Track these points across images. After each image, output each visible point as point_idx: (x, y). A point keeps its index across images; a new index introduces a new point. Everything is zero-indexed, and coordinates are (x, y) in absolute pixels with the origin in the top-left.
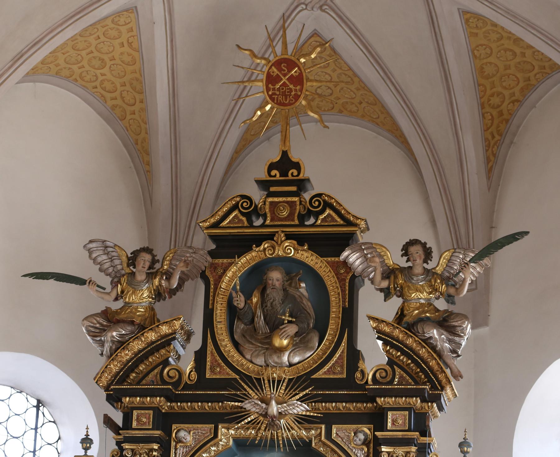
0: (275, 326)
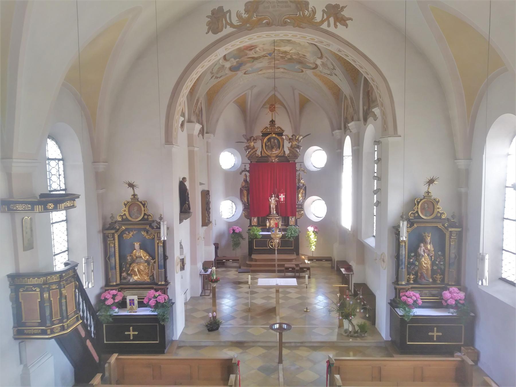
0: (272, 148)
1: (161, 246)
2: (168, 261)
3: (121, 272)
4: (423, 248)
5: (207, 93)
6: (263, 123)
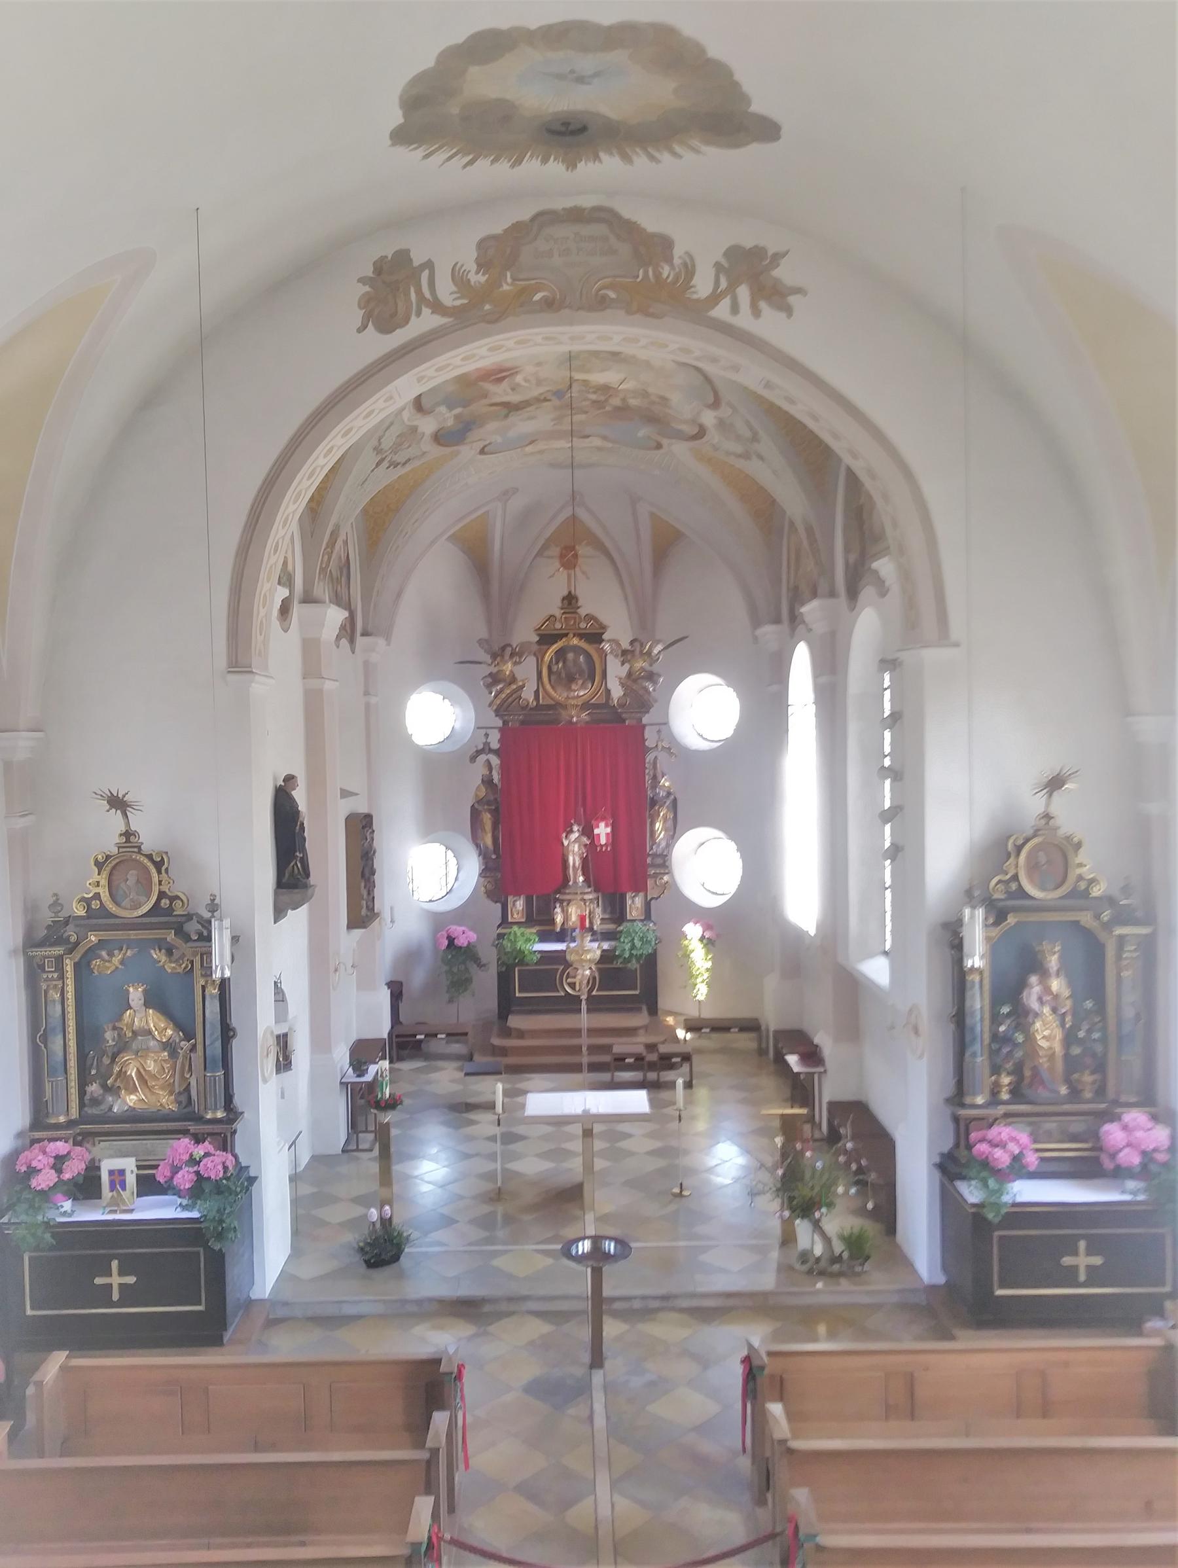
0: (571, 679)
1: (211, 995)
2: (235, 1043)
3: (83, 1081)
5: (365, 511)
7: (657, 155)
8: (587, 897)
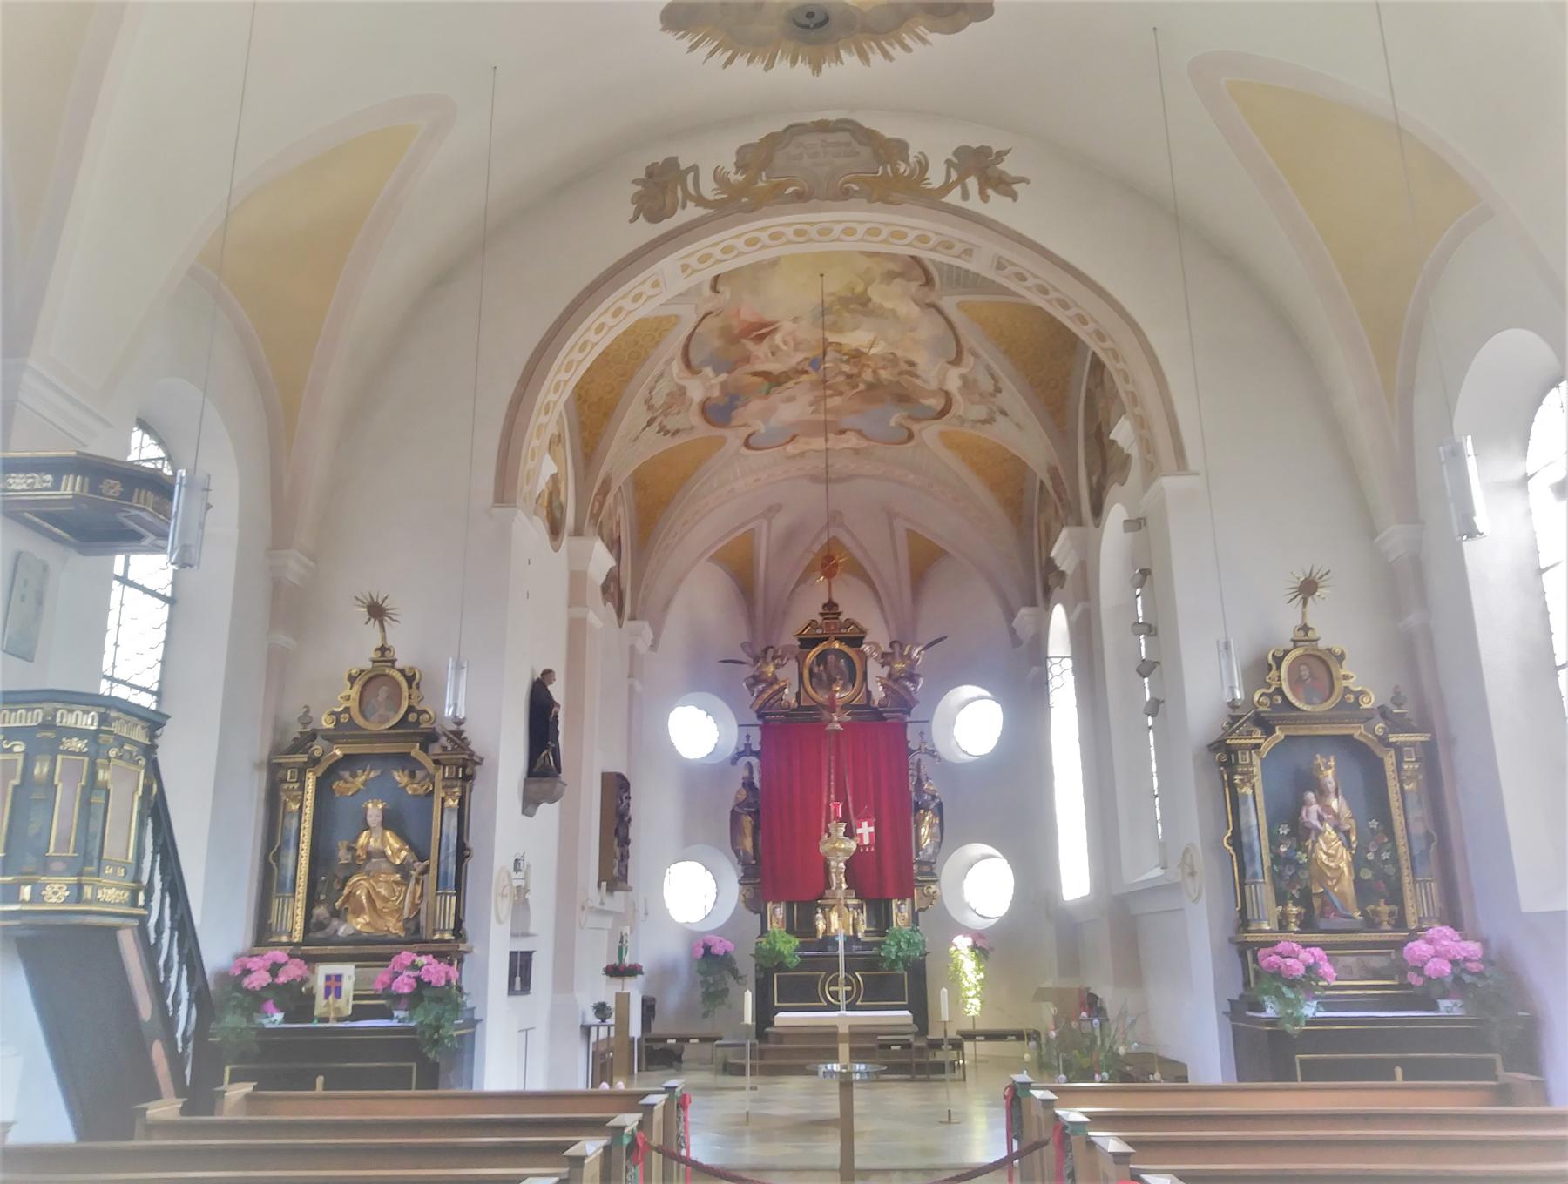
0: (832, 681)
1: (451, 808)
2: (471, 864)
4: (1315, 808)
5: (635, 472)
6: (808, 609)
7: (889, 48)
8: (850, 902)
